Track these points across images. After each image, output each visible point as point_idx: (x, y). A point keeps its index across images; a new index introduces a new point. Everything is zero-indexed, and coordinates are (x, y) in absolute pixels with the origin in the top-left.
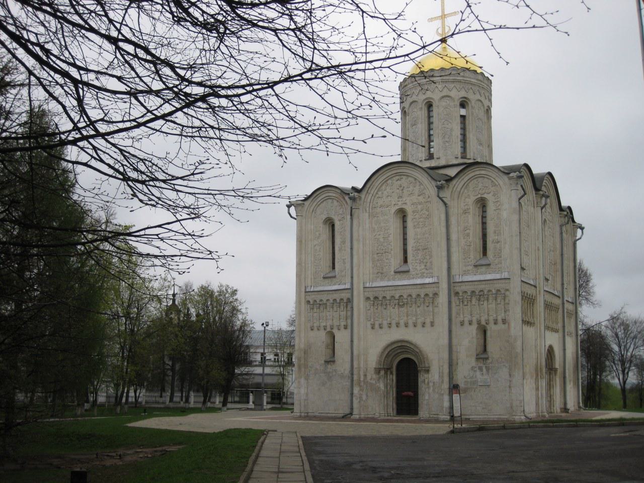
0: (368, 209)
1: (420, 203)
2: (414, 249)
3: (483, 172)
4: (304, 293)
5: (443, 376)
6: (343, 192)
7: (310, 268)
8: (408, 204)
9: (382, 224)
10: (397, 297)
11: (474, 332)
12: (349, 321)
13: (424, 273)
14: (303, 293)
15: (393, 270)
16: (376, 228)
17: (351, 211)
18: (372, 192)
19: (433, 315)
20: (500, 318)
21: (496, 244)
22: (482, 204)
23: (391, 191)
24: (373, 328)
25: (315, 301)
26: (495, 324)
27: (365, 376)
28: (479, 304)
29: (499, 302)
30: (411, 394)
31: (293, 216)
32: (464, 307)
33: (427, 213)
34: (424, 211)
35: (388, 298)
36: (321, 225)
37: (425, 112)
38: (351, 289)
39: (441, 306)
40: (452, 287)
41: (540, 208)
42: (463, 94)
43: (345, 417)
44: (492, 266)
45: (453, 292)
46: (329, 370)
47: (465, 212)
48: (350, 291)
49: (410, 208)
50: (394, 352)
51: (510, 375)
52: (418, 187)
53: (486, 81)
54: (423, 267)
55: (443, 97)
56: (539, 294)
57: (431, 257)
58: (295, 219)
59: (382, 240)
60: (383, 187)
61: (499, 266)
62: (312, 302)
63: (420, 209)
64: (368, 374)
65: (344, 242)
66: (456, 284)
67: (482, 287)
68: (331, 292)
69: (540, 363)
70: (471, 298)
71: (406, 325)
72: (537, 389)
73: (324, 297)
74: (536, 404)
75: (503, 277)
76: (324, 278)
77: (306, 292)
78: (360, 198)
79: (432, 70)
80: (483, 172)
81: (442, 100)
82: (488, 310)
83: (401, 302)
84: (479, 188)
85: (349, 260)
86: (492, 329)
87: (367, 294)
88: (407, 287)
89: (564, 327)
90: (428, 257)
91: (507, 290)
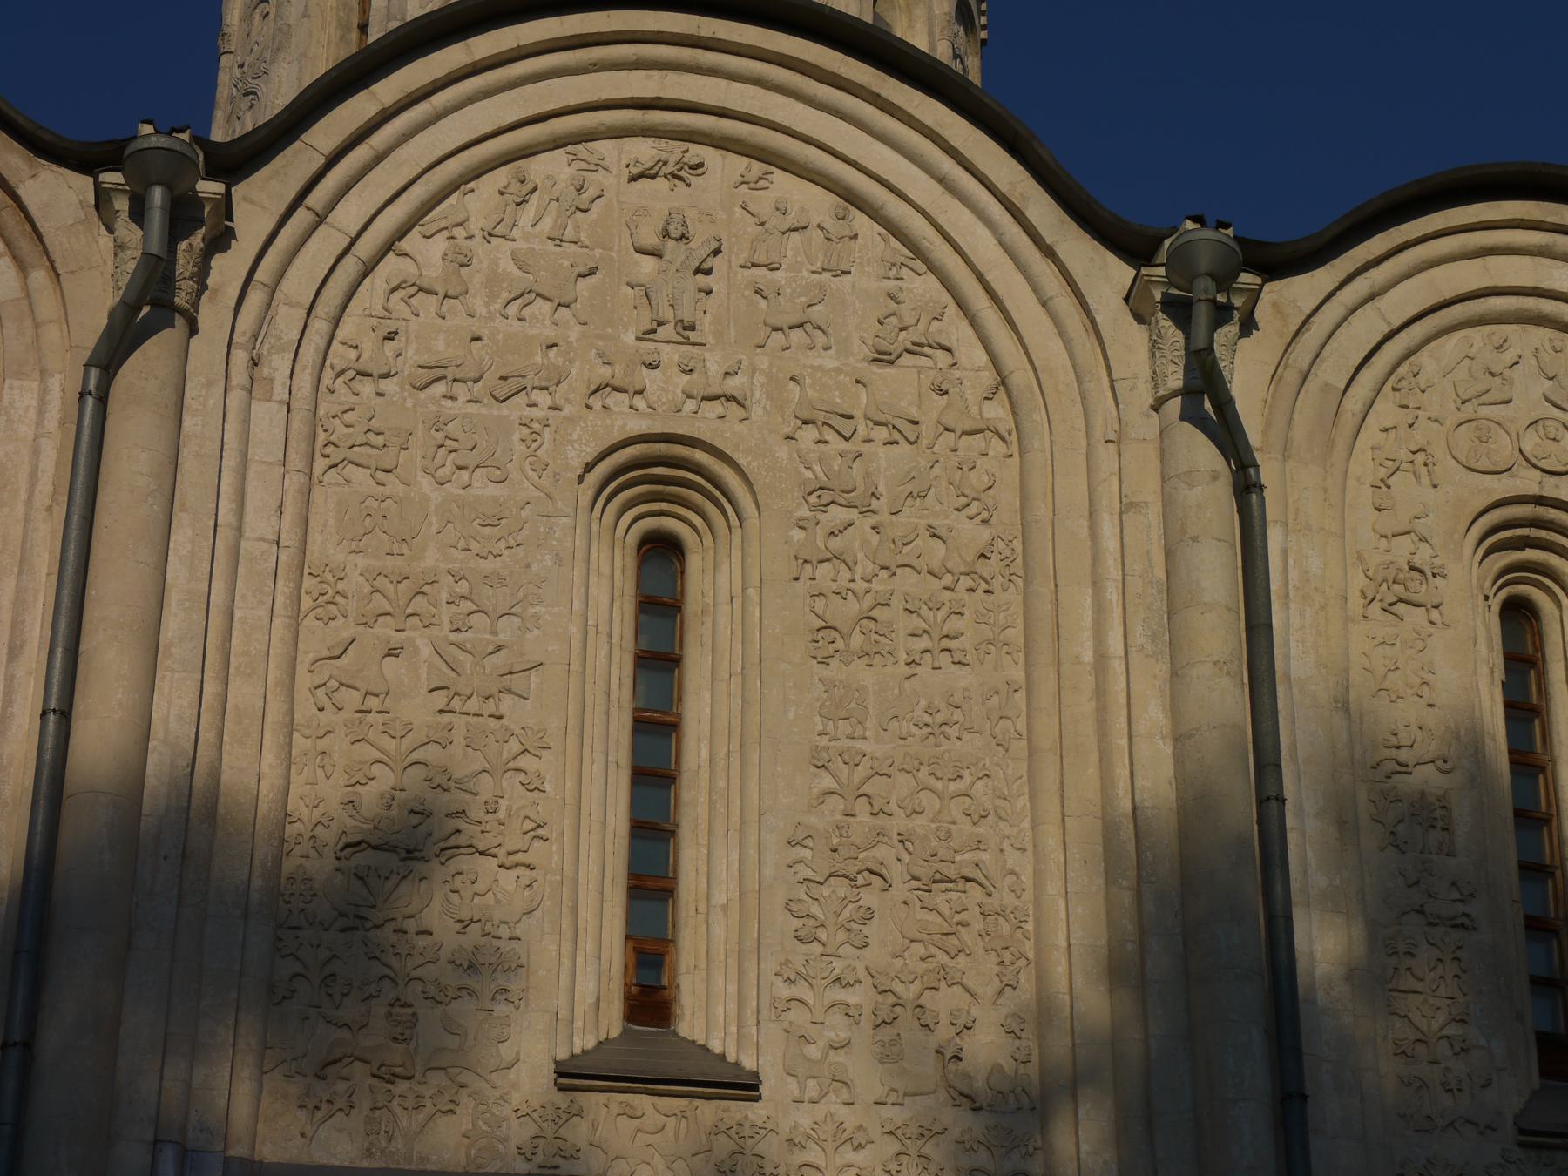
0: (278, 365)
1: (902, 430)
8: (757, 412)
9: (431, 558)
16: (355, 582)
33: (971, 534)
49: (783, 452)
52: (866, 282)
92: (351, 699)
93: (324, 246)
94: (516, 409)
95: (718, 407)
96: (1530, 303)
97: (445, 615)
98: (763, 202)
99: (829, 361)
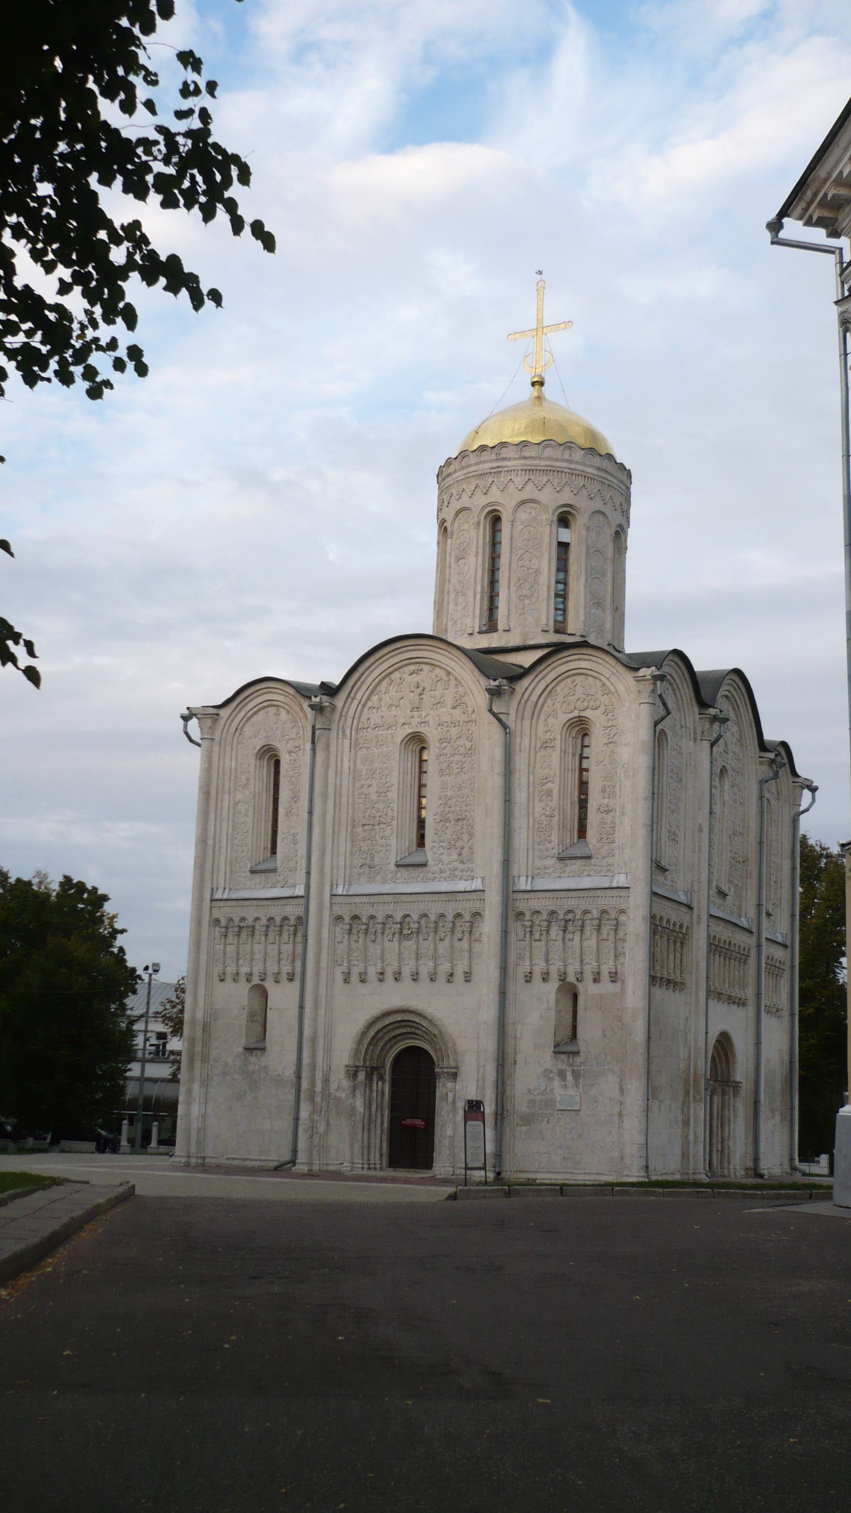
0: (348, 731)
1: (455, 724)
2: (438, 818)
3: (584, 664)
5: (483, 1088)
6: (303, 691)
7: (224, 850)
9: (377, 765)
10: (398, 918)
11: (553, 997)
12: (298, 965)
13: (455, 869)
15: (393, 860)
16: (364, 773)
17: (313, 734)
18: (359, 696)
19: (470, 958)
20: (605, 970)
22: (580, 728)
23: (400, 695)
24: (346, 981)
25: (231, 920)
26: (596, 980)
27: (326, 1081)
28: (564, 939)
29: (604, 936)
30: (419, 1122)
31: (193, 738)
32: (534, 944)
33: (468, 744)
36: (252, 761)
38: (306, 897)
39: (486, 940)
40: (510, 901)
41: (707, 745)
42: (566, 497)
43: (279, 1169)
44: (592, 861)
45: (510, 913)
46: (251, 1068)
47: (545, 745)
48: (302, 901)
49: (435, 732)
50: (387, 1033)
51: (622, 1090)
53: (619, 475)
54: (455, 857)
55: (523, 502)
56: (698, 923)
57: (471, 835)
58: (199, 745)
59: (374, 797)
61: (610, 860)
63: (454, 737)
64: (332, 1078)
65: (295, 798)
66: (520, 896)
67: (571, 903)
68: (265, 903)
69: (695, 1074)
70: (548, 927)
71: (415, 978)
72: (686, 1123)
74: (683, 1155)
75: (614, 885)
76: (253, 872)
77: (212, 900)
78: (333, 708)
79: (503, 445)
80: (584, 664)
81: (522, 508)
82: (579, 952)
83: (405, 929)
84: (576, 697)
85: (305, 835)
86: (588, 990)
87: (338, 911)
88: (420, 897)
89: (758, 995)
90: (465, 837)
91: (623, 911)
92: (363, 796)
93: (356, 702)
94: (389, 732)
95: (423, 725)
96: (578, 671)
97: (378, 777)
98: (433, 675)
99: (444, 710)
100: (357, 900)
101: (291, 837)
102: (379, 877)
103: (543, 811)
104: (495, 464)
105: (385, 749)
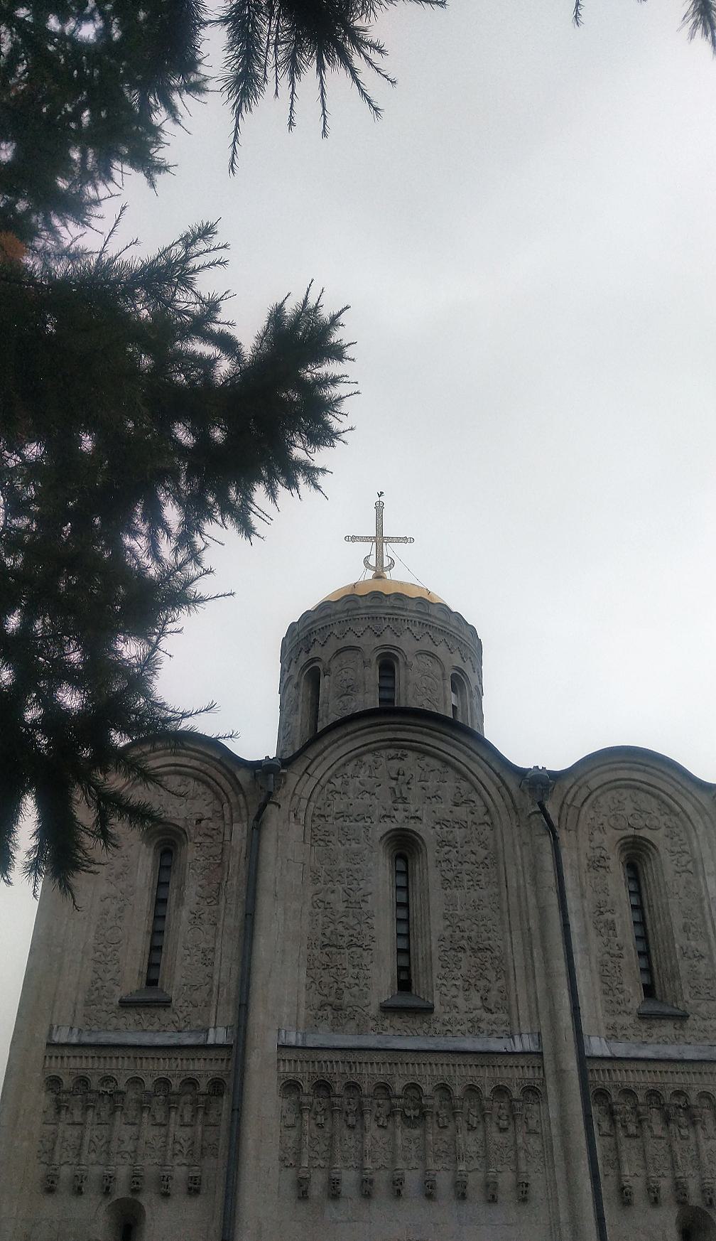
0: (302, 815)
4: (44, 1045)
10: (398, 1087)
13: (479, 1020)
14: (40, 1049)
21: (694, 962)
24: (303, 1196)
33: (483, 853)
34: (475, 847)
35: (367, 1088)
37: (373, 674)
44: (690, 1022)
49: (432, 831)
54: (479, 1003)
55: (421, 653)
59: (341, 907)
60: (349, 769)
62: (67, 1082)
66: (596, 1066)
67: (678, 1080)
68: (152, 1054)
71: (429, 1193)
73: (122, 1068)
77: (48, 1044)
90: (491, 975)
94: (361, 824)
98: (423, 764)
100: (325, 1056)
101: (200, 955)
102: (352, 1024)
103: (607, 949)
104: (390, 611)
105: (354, 845)
